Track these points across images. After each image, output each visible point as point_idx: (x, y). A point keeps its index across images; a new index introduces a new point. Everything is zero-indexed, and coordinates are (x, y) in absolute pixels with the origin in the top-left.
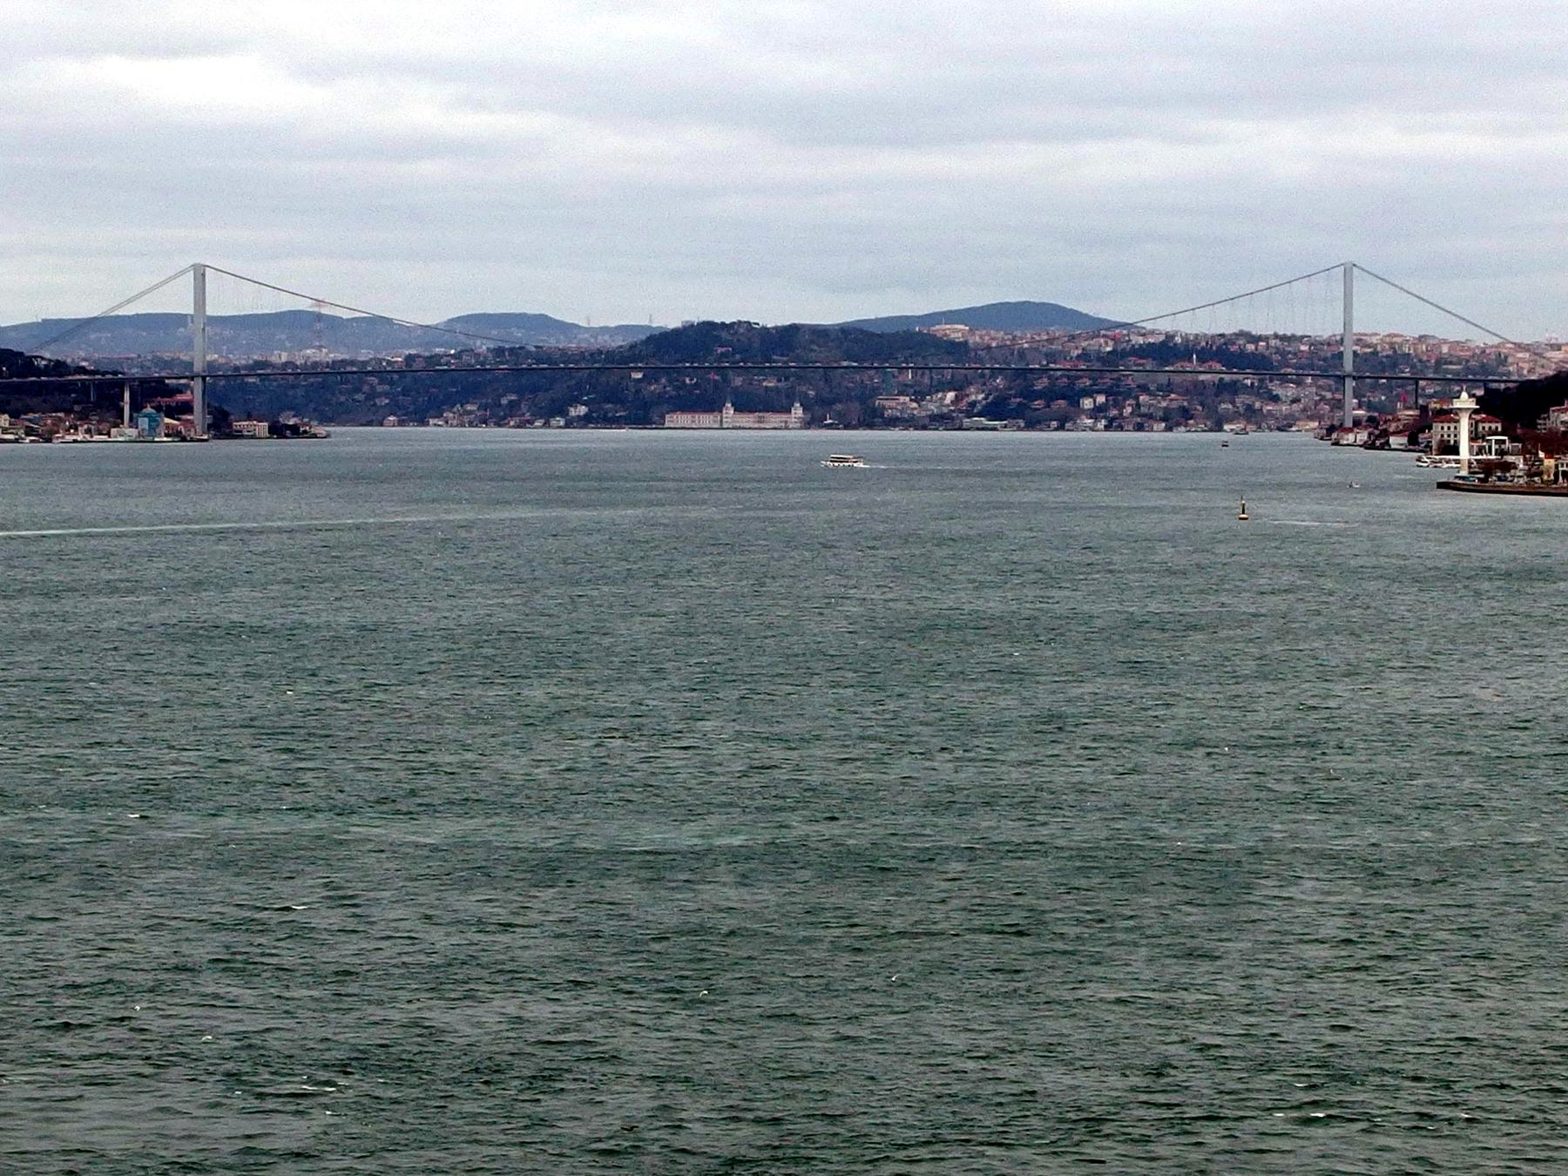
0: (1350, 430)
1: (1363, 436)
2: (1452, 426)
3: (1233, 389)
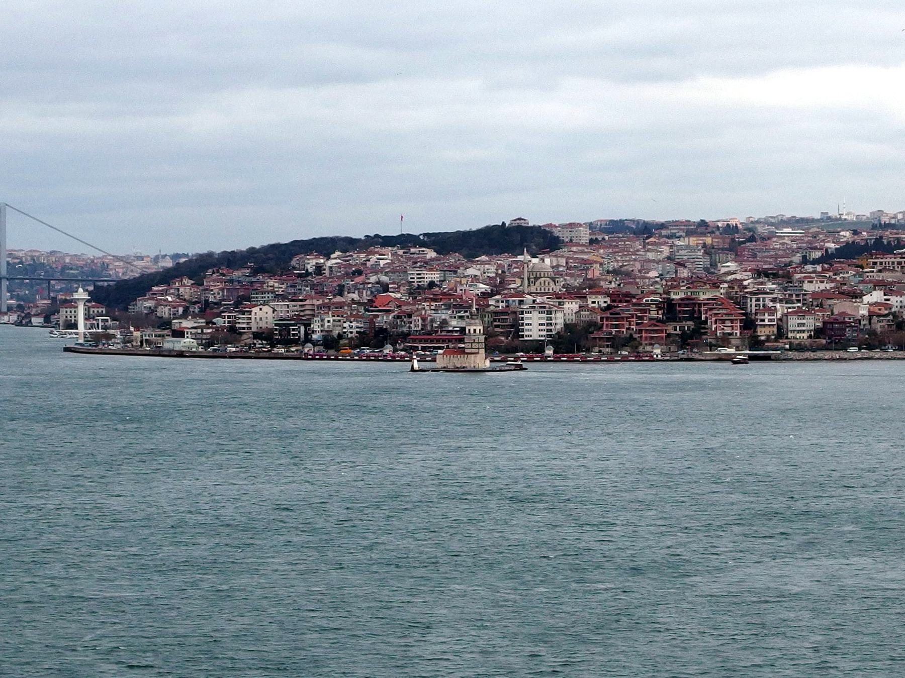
0: (6, 314)
1: (14, 317)
2: (73, 310)
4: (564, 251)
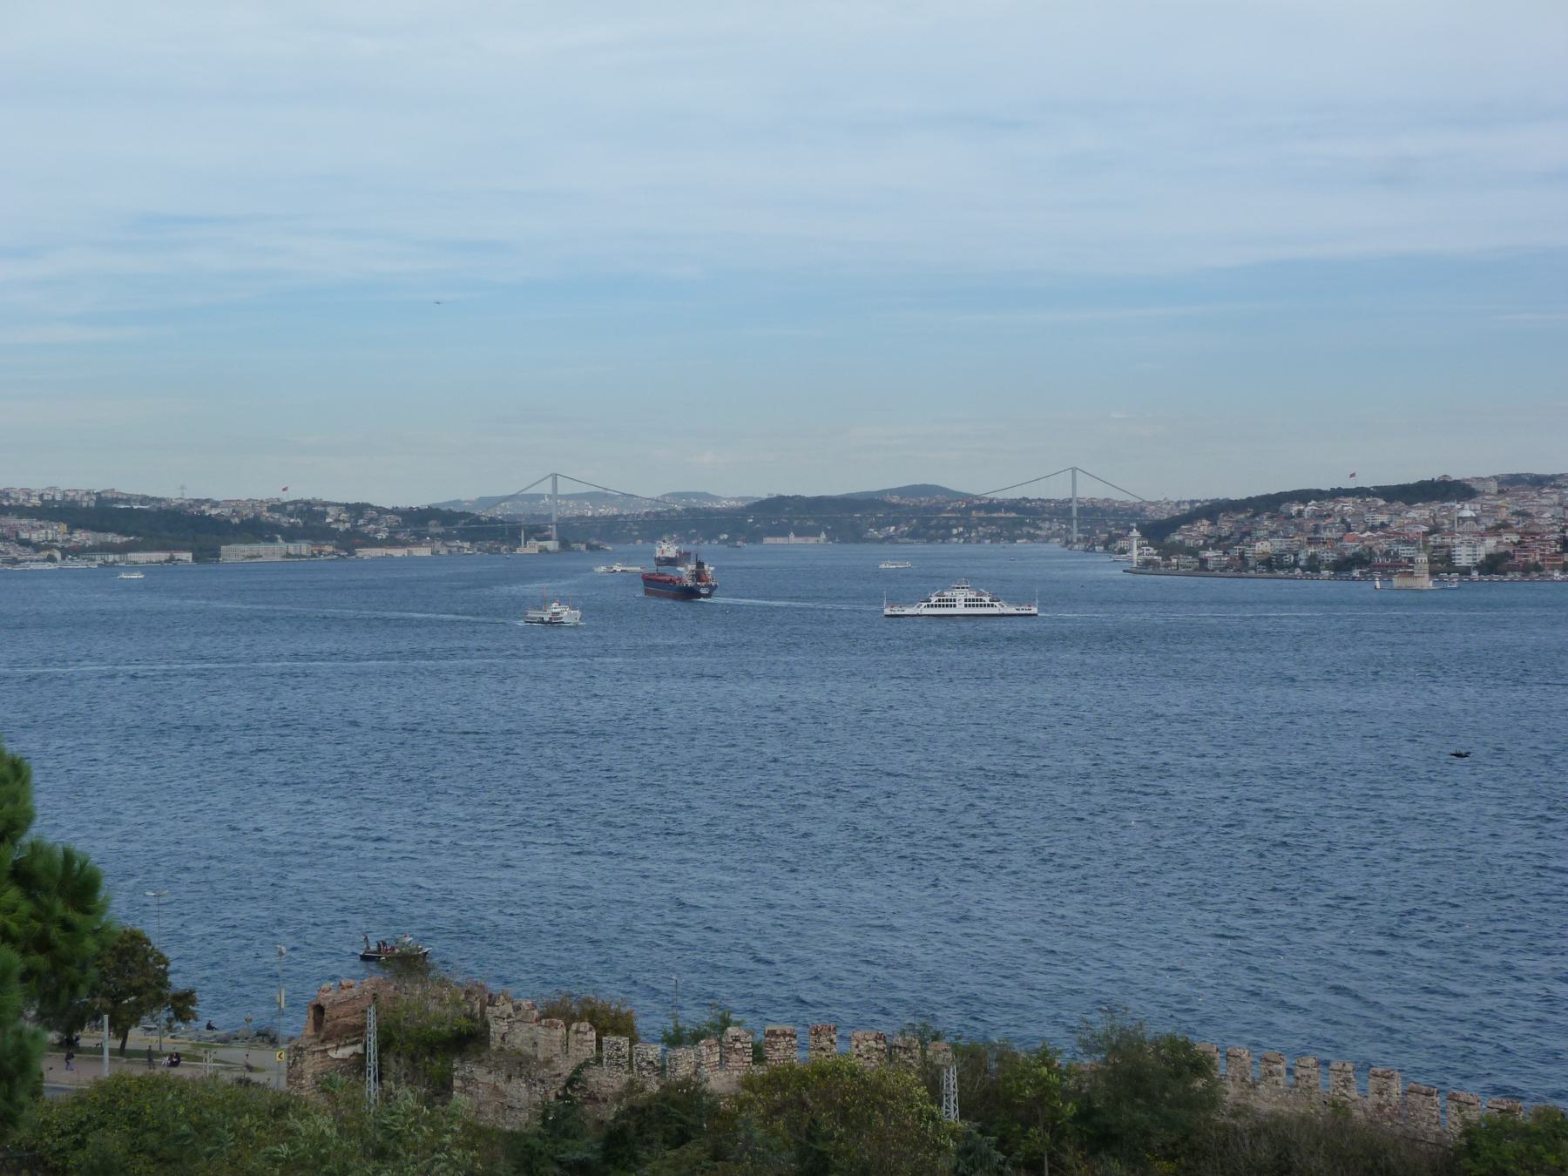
1: (1082, 546)
3: (1022, 523)
4: (1479, 498)
